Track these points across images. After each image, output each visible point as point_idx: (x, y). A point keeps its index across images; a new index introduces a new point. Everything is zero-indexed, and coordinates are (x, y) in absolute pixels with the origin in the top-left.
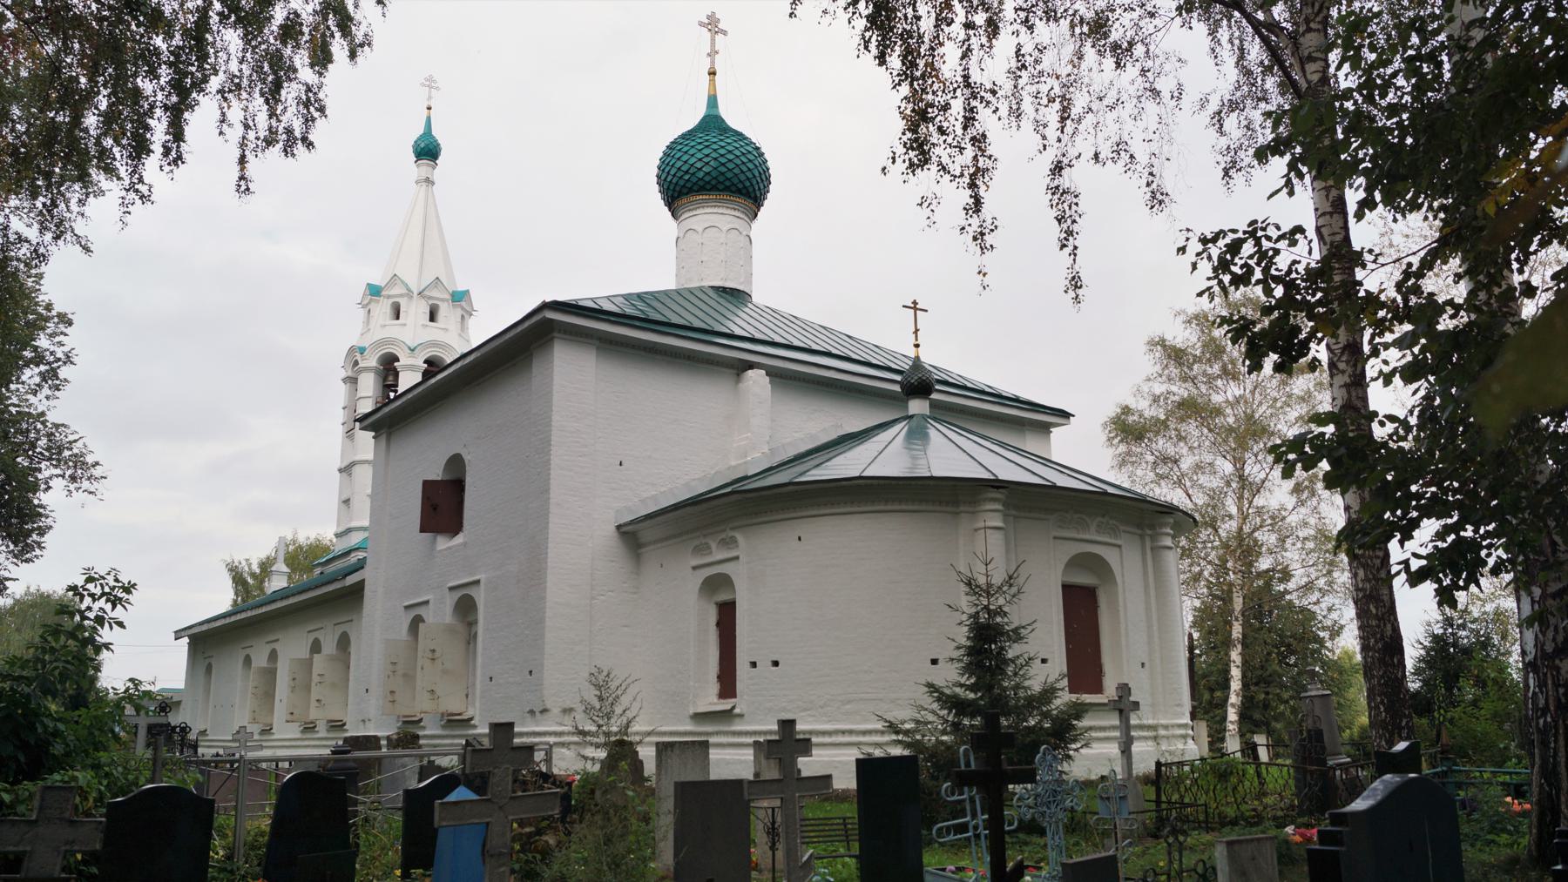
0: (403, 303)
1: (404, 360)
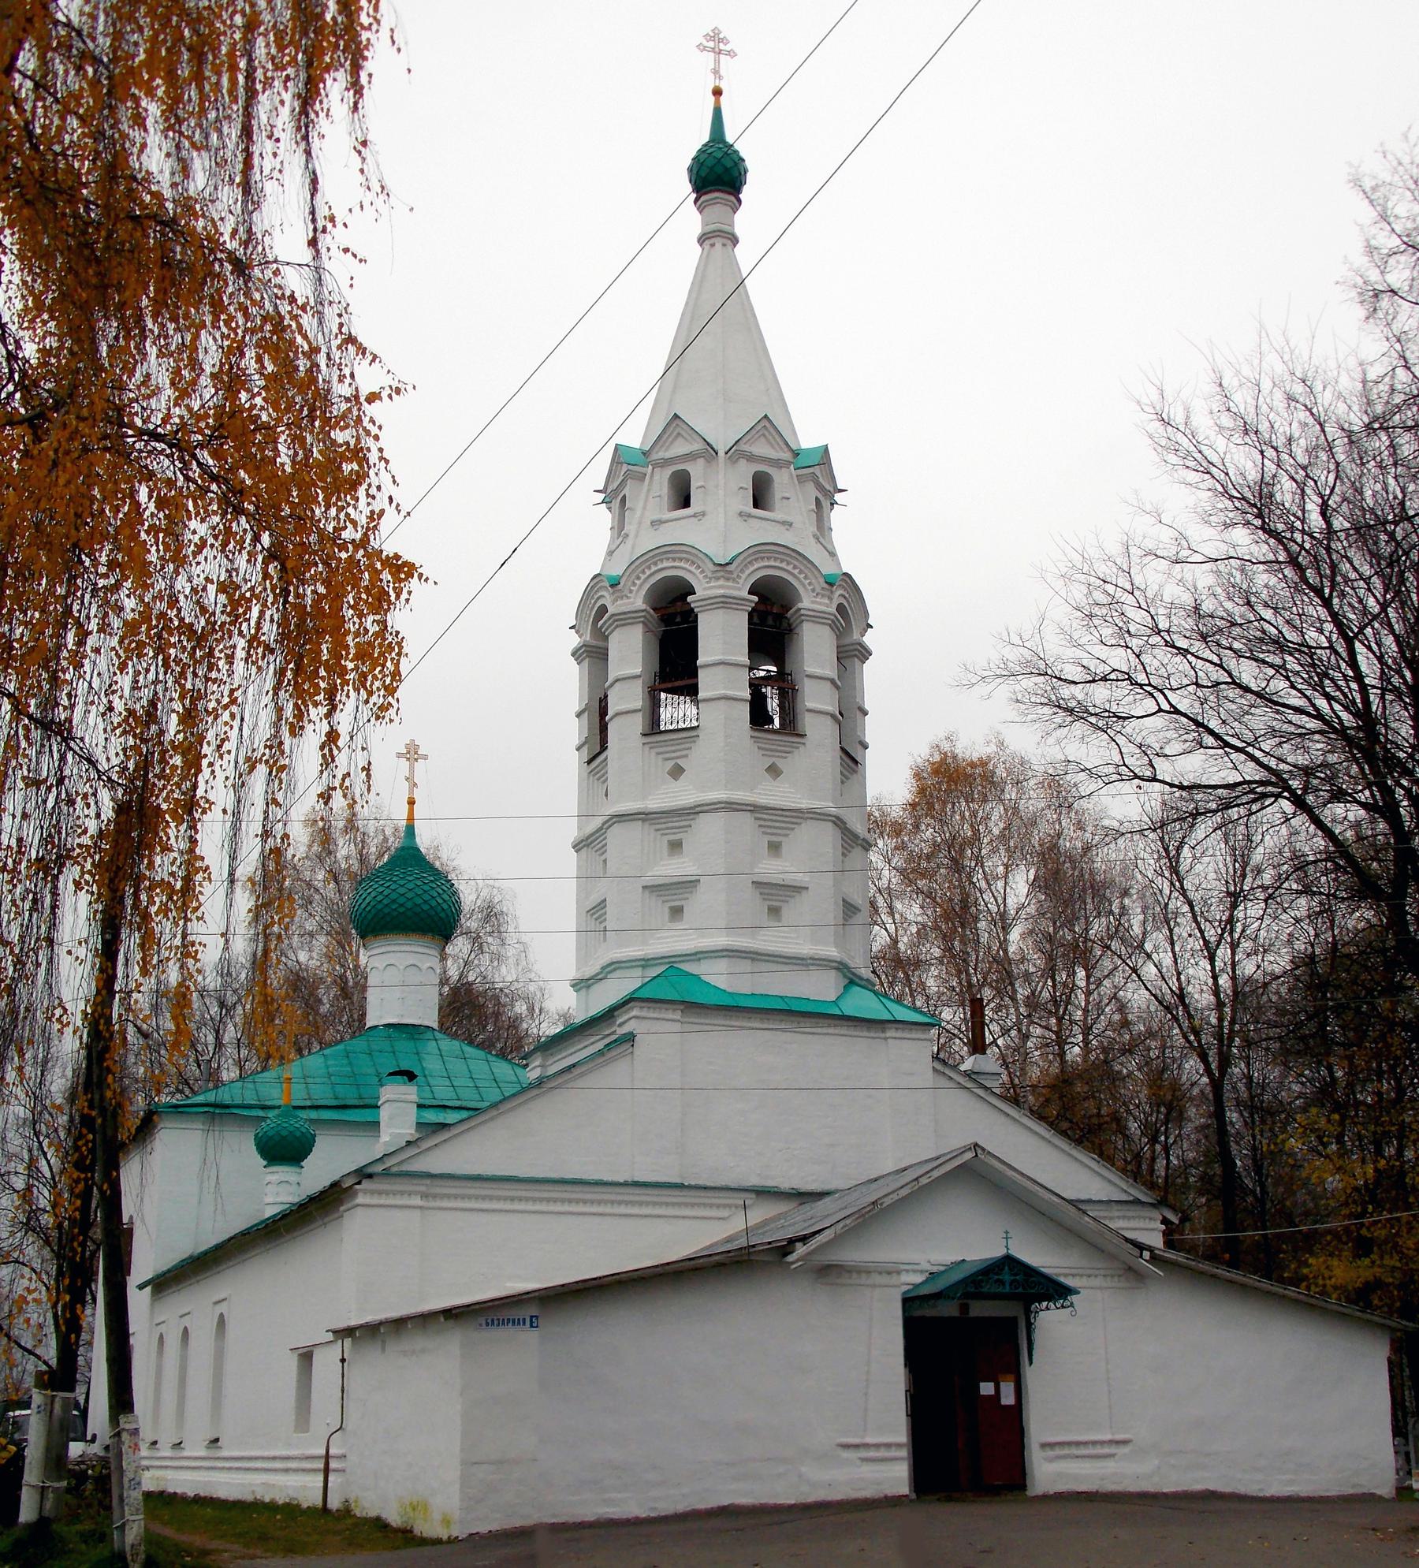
0: (696, 471)
1: (704, 589)
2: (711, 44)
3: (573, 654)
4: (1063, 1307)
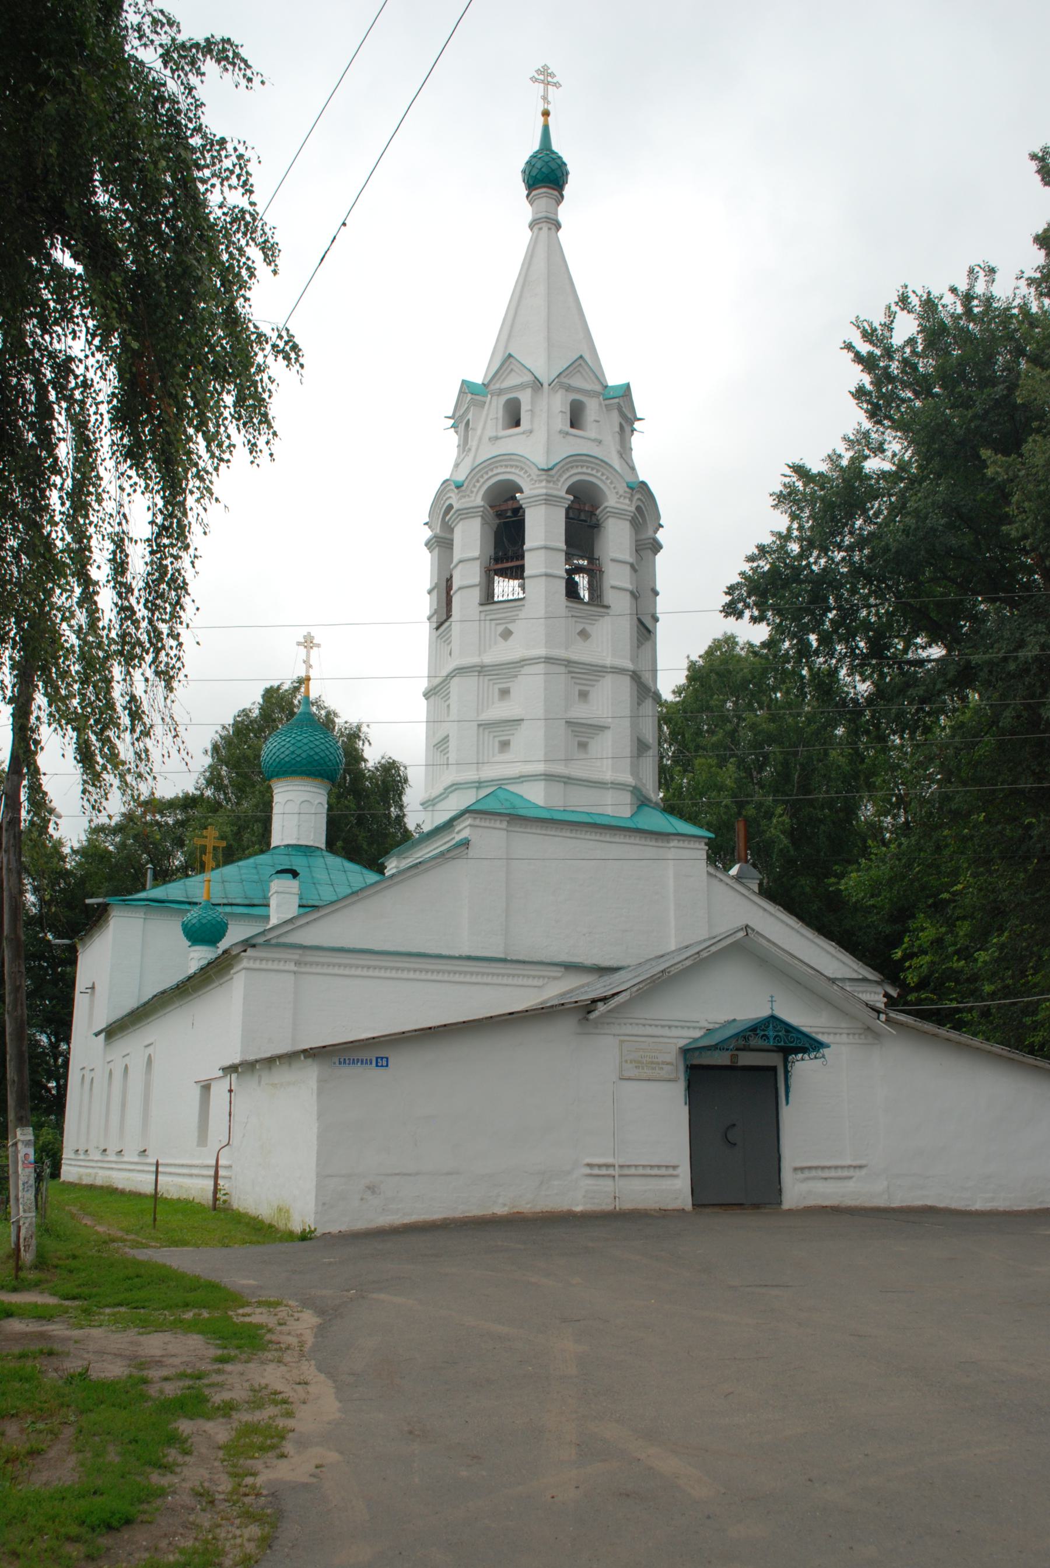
0: (525, 398)
1: (530, 490)
2: (541, 77)
3: (426, 545)
4: (816, 1058)
